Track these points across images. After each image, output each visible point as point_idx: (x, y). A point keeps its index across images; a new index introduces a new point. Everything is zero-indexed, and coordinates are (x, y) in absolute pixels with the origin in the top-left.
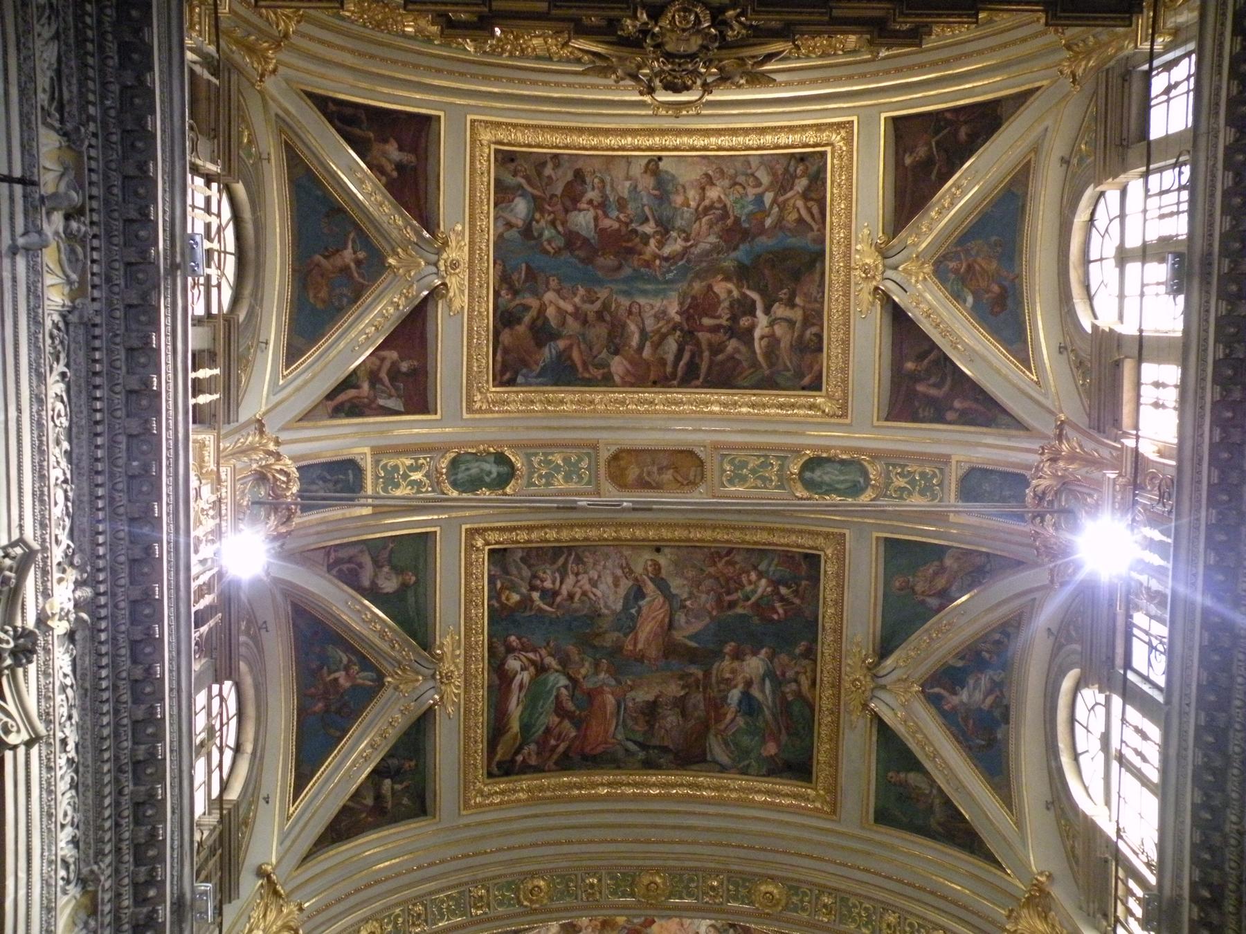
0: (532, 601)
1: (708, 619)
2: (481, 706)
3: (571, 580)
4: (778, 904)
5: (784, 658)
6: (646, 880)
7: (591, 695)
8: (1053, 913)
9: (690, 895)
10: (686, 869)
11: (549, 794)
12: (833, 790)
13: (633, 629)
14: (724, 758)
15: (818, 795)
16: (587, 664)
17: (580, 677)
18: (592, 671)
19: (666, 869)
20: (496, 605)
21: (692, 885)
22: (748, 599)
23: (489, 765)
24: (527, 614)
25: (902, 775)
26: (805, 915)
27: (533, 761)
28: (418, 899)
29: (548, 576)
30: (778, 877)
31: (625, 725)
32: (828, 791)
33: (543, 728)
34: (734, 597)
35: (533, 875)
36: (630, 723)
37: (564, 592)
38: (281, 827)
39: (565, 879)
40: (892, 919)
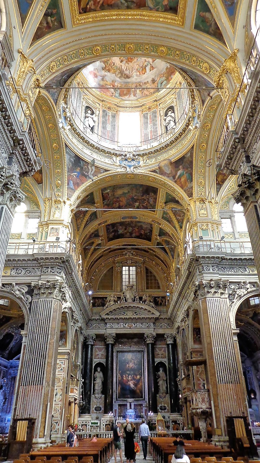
4: (164, 53)
6: (128, 46)
8: (236, 61)
9: (140, 50)
10: (140, 43)
11: (99, 19)
12: (183, 18)
14: (151, 6)
15: (179, 19)
19: (134, 43)
21: (141, 47)
23: (79, 10)
25: (204, 14)
26: (172, 57)
27: (93, 7)
28: (65, 55)
30: (165, 46)
32: (182, 18)
35: (96, 45)
38: (21, 37)
39: (105, 46)
40: (194, 59)
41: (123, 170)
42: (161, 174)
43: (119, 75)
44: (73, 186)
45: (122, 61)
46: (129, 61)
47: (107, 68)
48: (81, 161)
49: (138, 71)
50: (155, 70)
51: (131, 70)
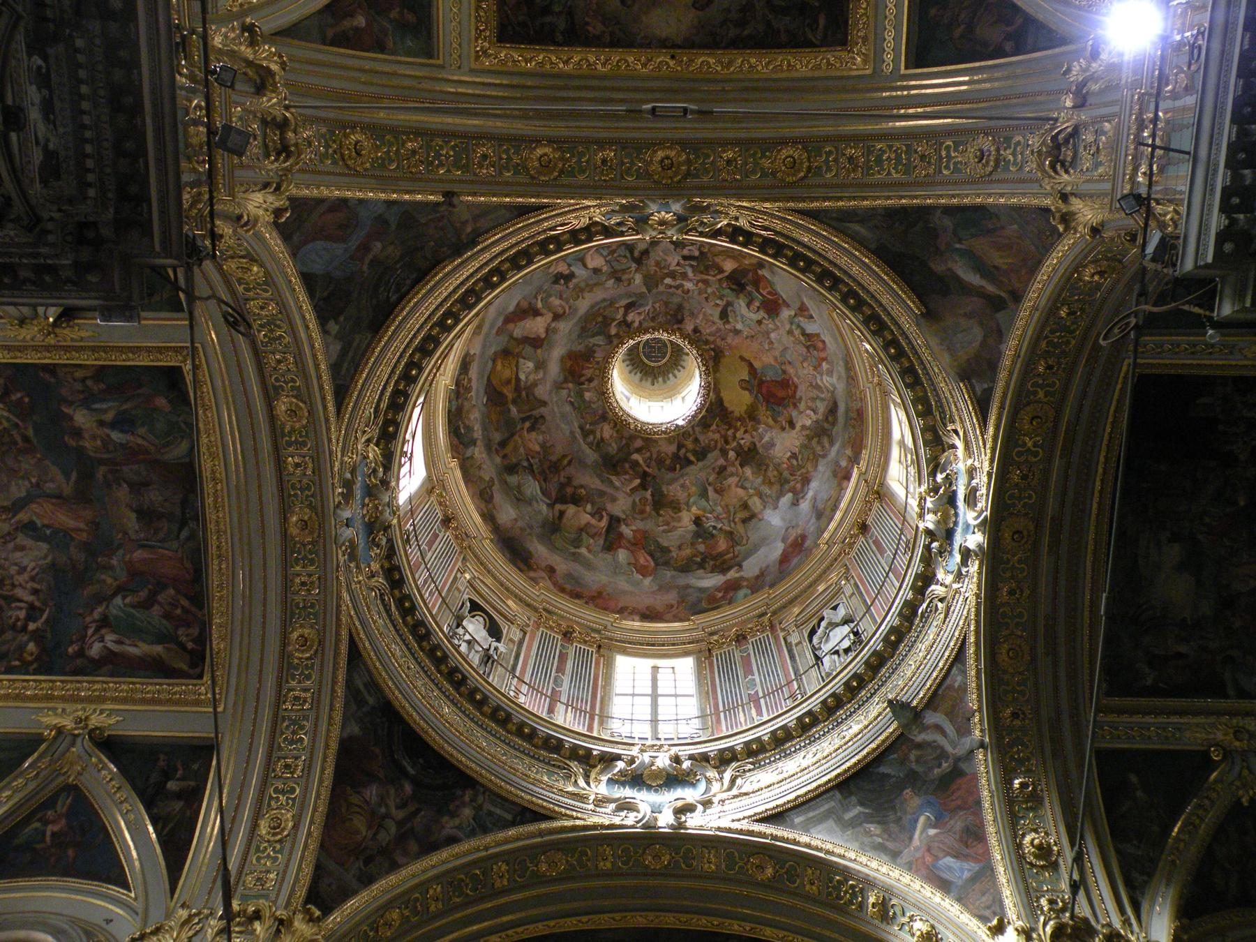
0: (37, 629)
1: (47, 462)
2: (124, 686)
3: (19, 592)
5: (64, 392)
7: (135, 573)
13: (66, 533)
14: (184, 446)
16: (103, 577)
17: (115, 584)
18: (110, 573)
20: (35, 666)
22: (16, 425)
23: (189, 677)
24: (49, 635)
27: (195, 631)
29: (14, 613)
31: (162, 541)
33: (164, 622)
34: (19, 440)
36: (161, 535)
37: (31, 598)
41: (974, 567)
42: (993, 367)
43: (825, 441)
44: (966, 865)
45: (792, 425)
46: (794, 396)
47: (799, 486)
48: (884, 769)
49: (820, 365)
50: (805, 300)
51: (815, 393)
